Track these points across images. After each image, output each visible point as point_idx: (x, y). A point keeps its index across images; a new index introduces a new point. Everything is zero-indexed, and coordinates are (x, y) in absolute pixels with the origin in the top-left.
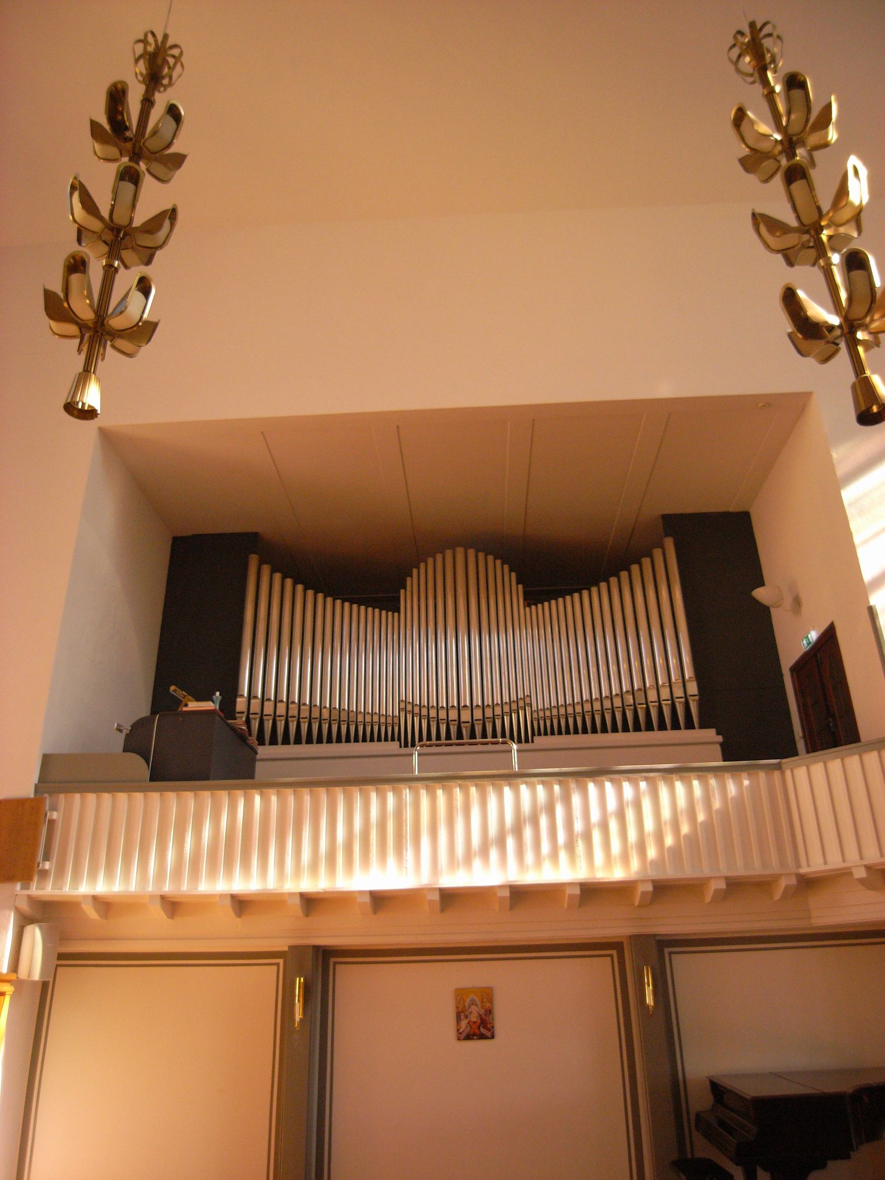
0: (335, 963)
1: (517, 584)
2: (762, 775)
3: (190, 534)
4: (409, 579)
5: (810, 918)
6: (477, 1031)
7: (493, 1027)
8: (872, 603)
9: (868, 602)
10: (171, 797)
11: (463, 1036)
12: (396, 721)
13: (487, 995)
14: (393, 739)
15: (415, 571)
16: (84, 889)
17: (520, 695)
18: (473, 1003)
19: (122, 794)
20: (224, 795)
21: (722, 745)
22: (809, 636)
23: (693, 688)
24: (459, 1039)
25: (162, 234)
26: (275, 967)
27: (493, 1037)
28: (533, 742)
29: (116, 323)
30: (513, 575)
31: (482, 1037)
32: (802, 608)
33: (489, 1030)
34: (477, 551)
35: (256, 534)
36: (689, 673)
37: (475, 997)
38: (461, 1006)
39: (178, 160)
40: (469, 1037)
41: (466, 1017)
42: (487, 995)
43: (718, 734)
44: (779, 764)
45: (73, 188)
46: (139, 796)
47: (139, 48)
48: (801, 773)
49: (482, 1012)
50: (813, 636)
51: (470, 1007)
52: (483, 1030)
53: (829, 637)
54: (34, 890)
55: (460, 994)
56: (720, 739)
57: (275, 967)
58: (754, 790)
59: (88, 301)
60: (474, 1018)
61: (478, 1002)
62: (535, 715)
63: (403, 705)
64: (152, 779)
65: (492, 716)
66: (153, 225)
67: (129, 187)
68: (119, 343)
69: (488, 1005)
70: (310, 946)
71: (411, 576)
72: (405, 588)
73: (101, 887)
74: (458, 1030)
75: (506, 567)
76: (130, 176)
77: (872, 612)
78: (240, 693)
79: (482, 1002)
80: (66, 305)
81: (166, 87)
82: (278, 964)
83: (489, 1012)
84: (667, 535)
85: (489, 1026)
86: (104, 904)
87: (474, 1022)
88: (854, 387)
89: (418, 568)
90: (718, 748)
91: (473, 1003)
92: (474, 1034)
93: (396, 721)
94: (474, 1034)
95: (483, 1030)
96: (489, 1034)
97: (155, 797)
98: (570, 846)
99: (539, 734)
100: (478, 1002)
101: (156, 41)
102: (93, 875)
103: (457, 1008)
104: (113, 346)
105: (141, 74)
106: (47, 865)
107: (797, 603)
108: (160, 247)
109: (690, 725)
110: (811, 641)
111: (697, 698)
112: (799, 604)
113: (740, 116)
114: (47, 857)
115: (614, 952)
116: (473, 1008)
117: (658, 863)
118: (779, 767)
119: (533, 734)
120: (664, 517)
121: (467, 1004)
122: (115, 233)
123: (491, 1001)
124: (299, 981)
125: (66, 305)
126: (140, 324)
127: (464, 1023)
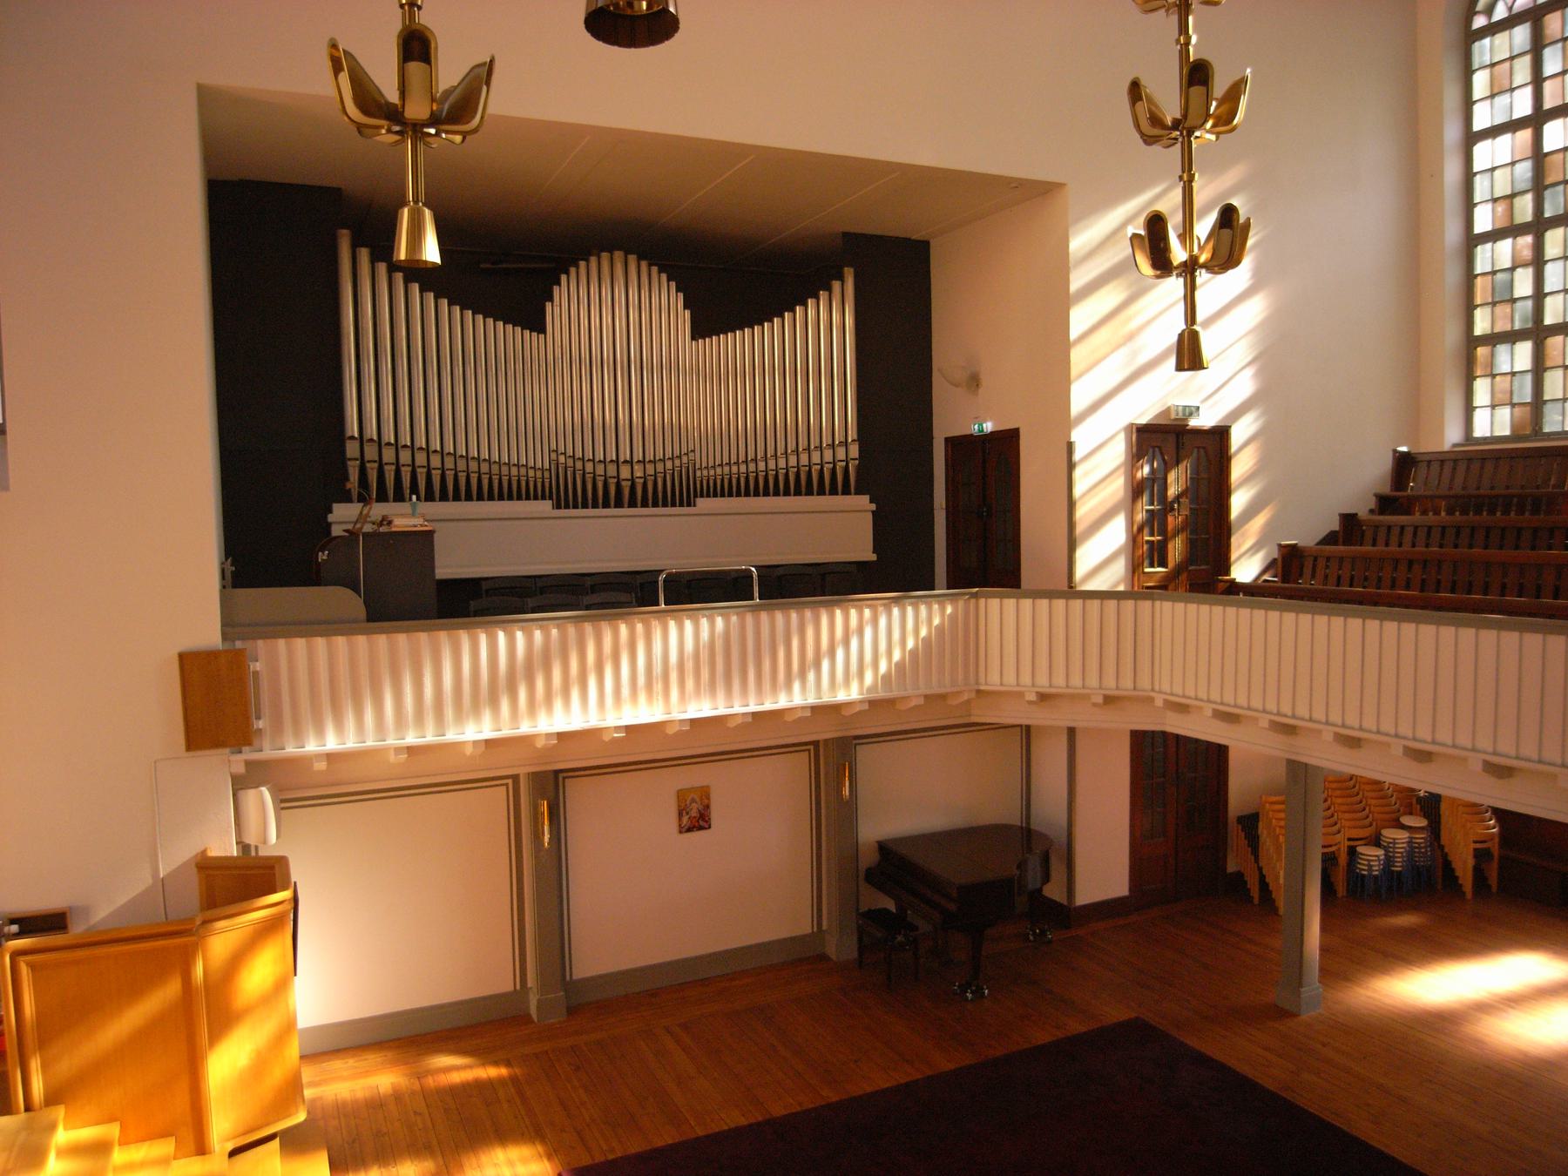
0: (564, 778)
1: (684, 309)
2: (961, 603)
3: (235, 178)
4: (556, 289)
5: (970, 715)
6: (696, 824)
7: (710, 819)
8: (1072, 440)
10: (402, 639)
11: (684, 830)
12: (547, 474)
13: (705, 793)
14: (543, 498)
15: (564, 278)
16: (311, 746)
17: (684, 450)
18: (693, 800)
19: (340, 638)
20: (464, 637)
21: (873, 512)
22: (984, 425)
23: (854, 451)
24: (681, 832)
26: (505, 787)
27: (710, 827)
28: (695, 506)
30: (681, 295)
31: (701, 828)
32: (980, 391)
33: (706, 822)
34: (640, 259)
35: (339, 189)
36: (852, 434)
37: (696, 797)
38: (683, 805)
40: (689, 830)
41: (687, 813)
42: (705, 793)
43: (871, 501)
44: (977, 592)
46: (361, 640)
48: (994, 603)
49: (701, 807)
50: (988, 427)
51: (690, 804)
52: (701, 823)
53: (1007, 441)
54: (249, 754)
55: (681, 795)
56: (873, 507)
57: (505, 787)
58: (953, 617)
60: (694, 813)
61: (698, 800)
62: (698, 473)
63: (554, 456)
64: (370, 619)
65: (653, 473)
69: (706, 801)
70: (550, 771)
71: (560, 285)
72: (552, 301)
73: (332, 743)
74: (680, 825)
75: (673, 285)
77: (1070, 447)
78: (349, 434)
79: (701, 799)
82: (507, 785)
83: (708, 807)
85: (707, 819)
86: (331, 757)
87: (695, 817)
88: (1181, 336)
89: (567, 273)
90: (870, 516)
91: (693, 800)
92: (694, 827)
93: (547, 474)
94: (694, 827)
95: (701, 823)
96: (707, 826)
97: (382, 640)
98: (803, 674)
99: (702, 496)
100: (698, 800)
102: (320, 732)
103: (679, 806)
106: (261, 724)
107: (974, 382)
109: (846, 492)
110: (985, 430)
111: (857, 462)
112: (977, 385)
114: (258, 718)
115: (812, 747)
116: (694, 804)
117: (873, 688)
118: (975, 596)
119: (695, 496)
120: (846, 235)
121: (688, 802)
123: (708, 799)
124: (544, 806)
127: (685, 819)
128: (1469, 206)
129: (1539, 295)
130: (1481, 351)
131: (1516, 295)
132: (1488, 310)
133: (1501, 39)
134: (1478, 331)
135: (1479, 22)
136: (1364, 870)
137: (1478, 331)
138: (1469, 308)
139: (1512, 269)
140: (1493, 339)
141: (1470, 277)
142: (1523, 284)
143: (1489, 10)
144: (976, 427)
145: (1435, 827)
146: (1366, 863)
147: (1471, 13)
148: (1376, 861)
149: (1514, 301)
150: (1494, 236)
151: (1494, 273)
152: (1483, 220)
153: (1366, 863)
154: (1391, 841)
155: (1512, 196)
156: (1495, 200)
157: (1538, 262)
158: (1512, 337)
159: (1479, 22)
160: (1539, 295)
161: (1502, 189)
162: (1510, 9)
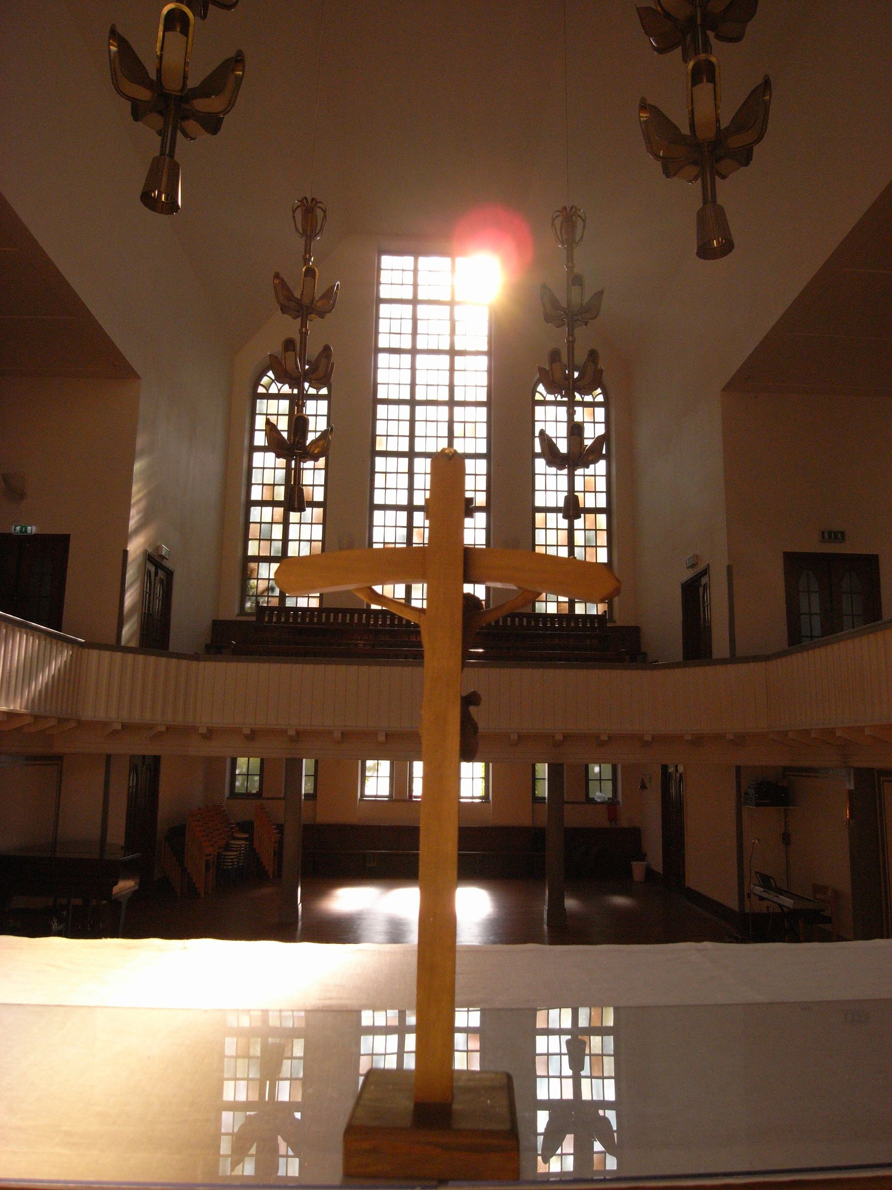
9: (126, 544)
22: (29, 528)
50: (32, 529)
128: (249, 485)
129: (285, 540)
130: (253, 565)
131: (273, 538)
132: (257, 542)
133: (273, 403)
134: (250, 553)
135: (261, 390)
136: (230, 865)
137: (250, 553)
138: (246, 540)
139: (272, 523)
140: (259, 559)
141: (247, 523)
142: (277, 532)
143: (267, 387)
144: (18, 528)
145: (250, 840)
146: (230, 860)
147: (257, 383)
148: (235, 858)
149: (271, 540)
150: (262, 503)
151: (261, 523)
152: (256, 494)
153: (230, 860)
154: (238, 846)
155: (274, 485)
156: (263, 485)
157: (286, 523)
158: (269, 559)
159: (261, 390)
160: (285, 540)
161: (268, 480)
162: (279, 390)
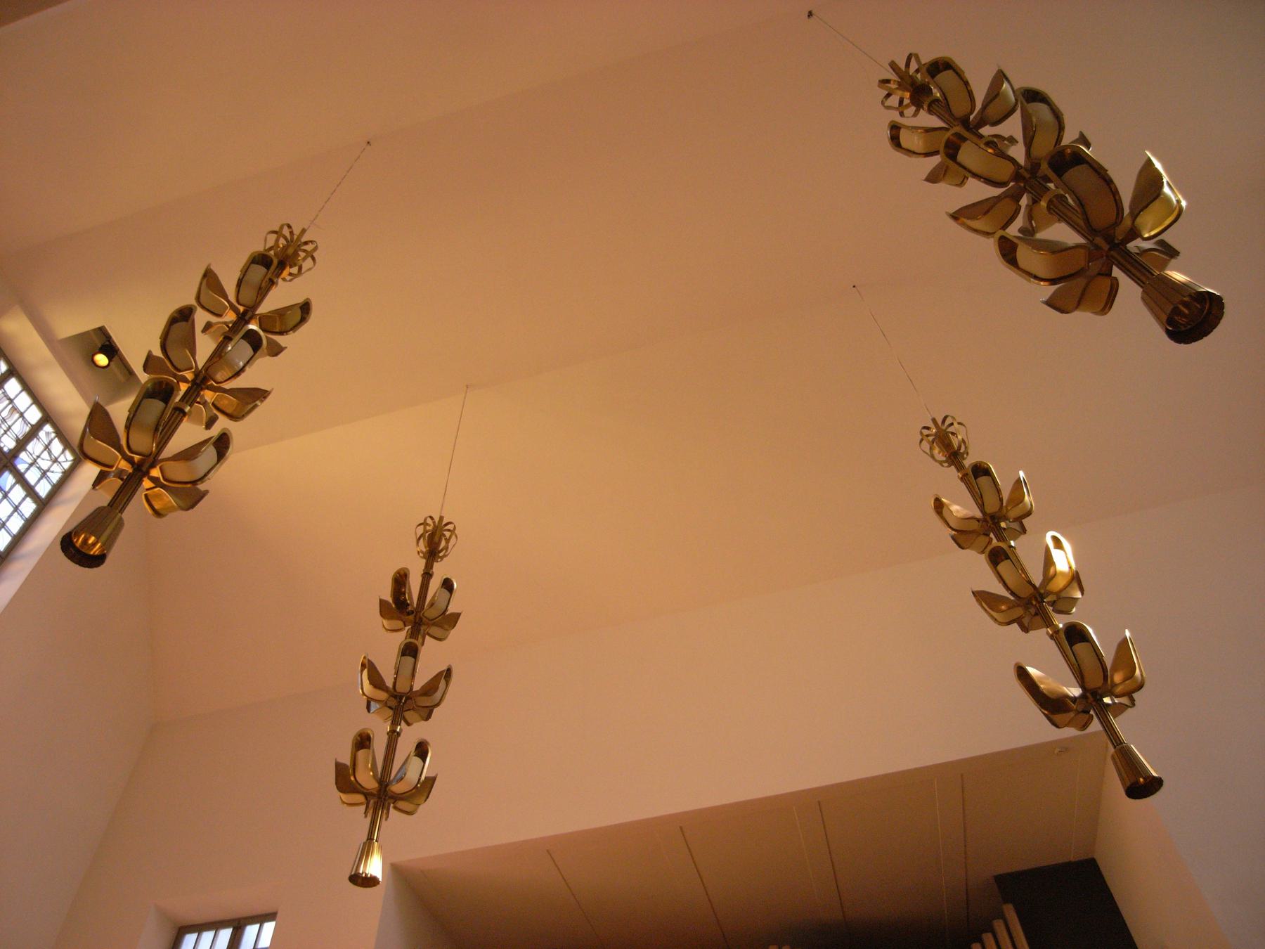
25: (438, 694)
29: (397, 788)
39: (456, 616)
45: (363, 666)
47: (420, 530)
59: (371, 773)
66: (430, 688)
67: (410, 660)
68: (401, 804)
76: (410, 651)
80: (352, 779)
81: (442, 558)
84: (1006, 901)
101: (434, 523)
104: (395, 808)
105: (422, 552)
108: (437, 705)
113: (939, 506)
122: (398, 700)
125: (352, 779)
126: (419, 785)
